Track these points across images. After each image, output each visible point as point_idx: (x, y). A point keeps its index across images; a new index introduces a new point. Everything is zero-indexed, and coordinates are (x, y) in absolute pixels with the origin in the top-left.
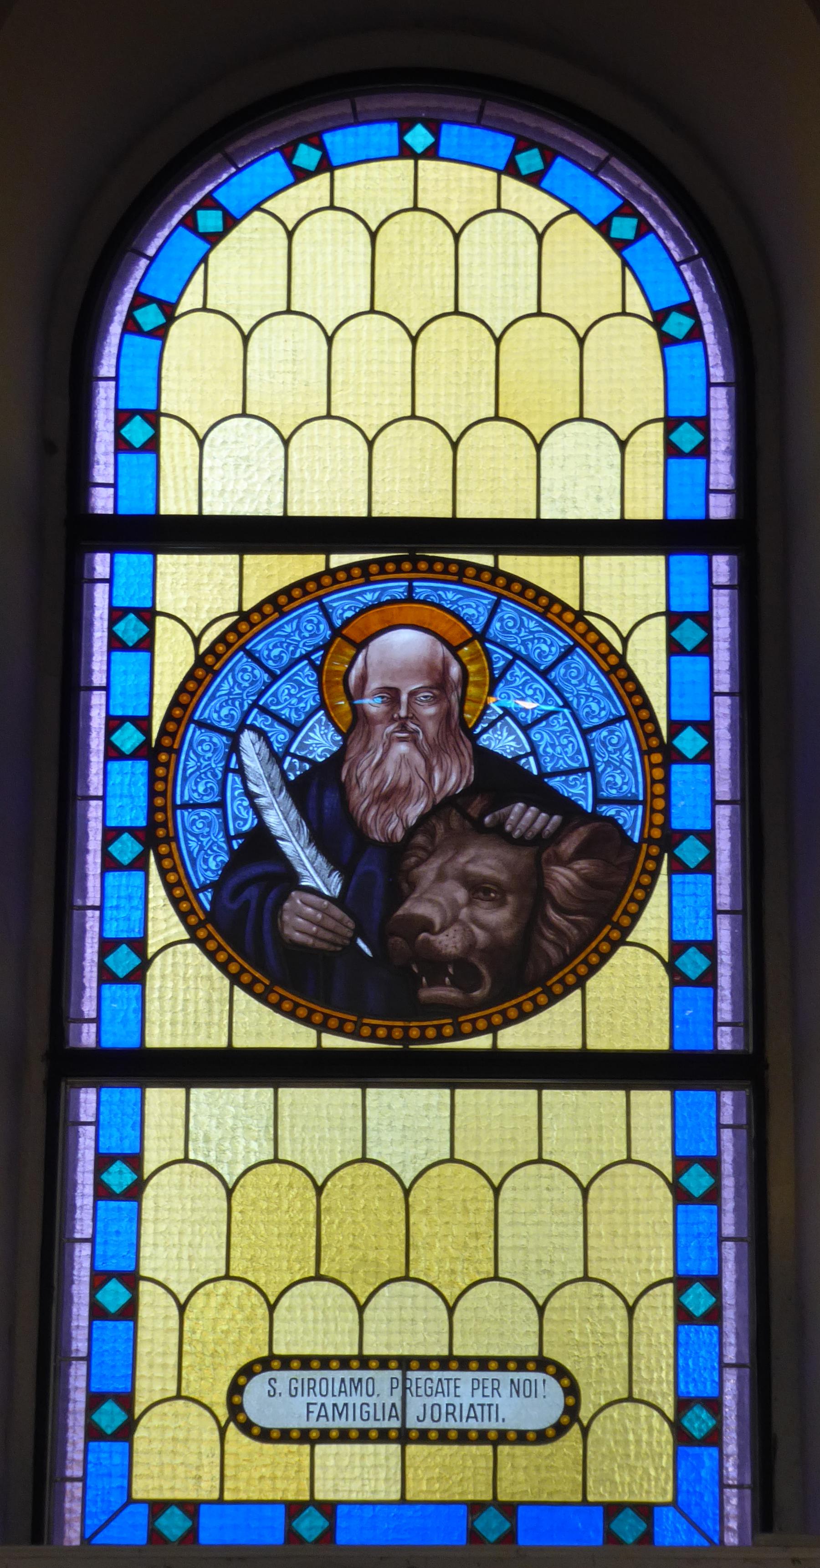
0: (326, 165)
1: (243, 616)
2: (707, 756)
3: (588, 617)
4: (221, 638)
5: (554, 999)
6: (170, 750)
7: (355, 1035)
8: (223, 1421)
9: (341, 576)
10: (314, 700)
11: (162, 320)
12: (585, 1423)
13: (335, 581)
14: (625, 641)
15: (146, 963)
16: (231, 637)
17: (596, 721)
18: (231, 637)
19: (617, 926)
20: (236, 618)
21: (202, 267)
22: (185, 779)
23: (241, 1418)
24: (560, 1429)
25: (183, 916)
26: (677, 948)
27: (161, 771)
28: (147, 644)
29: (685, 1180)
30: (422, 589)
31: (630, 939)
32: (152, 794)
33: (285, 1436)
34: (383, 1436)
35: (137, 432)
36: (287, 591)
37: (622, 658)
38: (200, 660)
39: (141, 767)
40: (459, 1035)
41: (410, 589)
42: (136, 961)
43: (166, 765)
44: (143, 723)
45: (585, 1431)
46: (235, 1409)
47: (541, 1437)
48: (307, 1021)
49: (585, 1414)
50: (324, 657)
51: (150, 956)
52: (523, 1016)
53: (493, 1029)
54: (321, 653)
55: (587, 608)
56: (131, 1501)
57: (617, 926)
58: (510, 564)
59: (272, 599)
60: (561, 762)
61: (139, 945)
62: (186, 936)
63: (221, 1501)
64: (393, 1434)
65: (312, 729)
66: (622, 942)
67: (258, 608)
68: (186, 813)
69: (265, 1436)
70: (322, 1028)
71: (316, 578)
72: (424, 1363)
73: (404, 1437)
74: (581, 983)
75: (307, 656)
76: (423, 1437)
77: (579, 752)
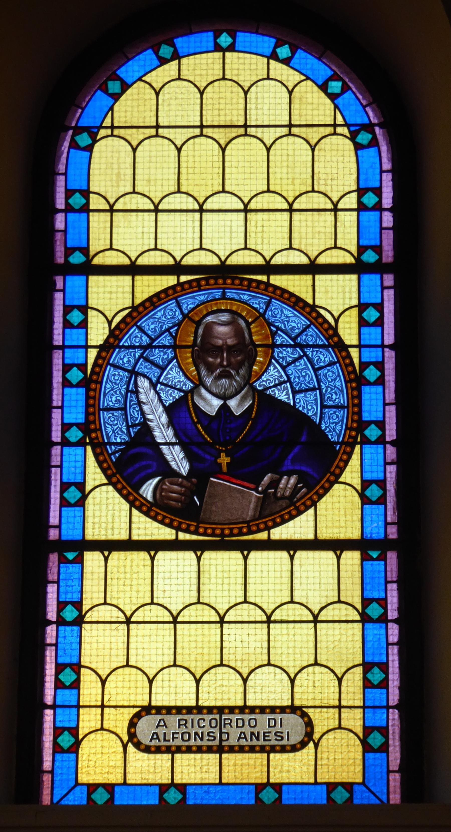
0: (176, 56)
1: (134, 308)
2: (381, 381)
3: (318, 309)
4: (123, 320)
5: (300, 513)
6: (97, 382)
7: (196, 532)
8: (125, 742)
9: (186, 286)
10: (172, 354)
11: (90, 142)
12: (316, 741)
13: (183, 289)
14: (337, 321)
15: (84, 497)
16: (128, 320)
17: (322, 364)
18: (128, 320)
19: (333, 474)
20: (130, 310)
21: (110, 112)
22: (105, 395)
23: (135, 740)
24: (303, 744)
25: (104, 471)
26: (366, 484)
27: (91, 402)
28: (84, 324)
29: (368, 611)
30: (230, 294)
31: (341, 480)
32: (87, 406)
33: (158, 750)
34: (210, 750)
35: (76, 317)
36: (157, 295)
37: (335, 330)
38: (112, 332)
39: (82, 391)
40: (250, 532)
41: (224, 293)
42: (79, 495)
43: (95, 390)
44: (82, 367)
45: (316, 746)
46: (132, 736)
47: (294, 749)
48: (170, 525)
49: (316, 736)
50: (177, 331)
51: (87, 492)
52: (284, 521)
53: (268, 529)
54: (176, 328)
55: (317, 303)
56: (77, 784)
57: (333, 474)
58: (276, 280)
59: (150, 299)
60: (303, 385)
61: (81, 486)
62: (105, 481)
63: (125, 783)
64: (215, 748)
65: (171, 369)
66: (336, 482)
67: (142, 304)
68: (105, 413)
69: (147, 750)
70: (178, 529)
71: (173, 287)
72: (232, 709)
73: (220, 750)
74: (314, 504)
75: (168, 330)
76: (232, 750)
77: (312, 379)
